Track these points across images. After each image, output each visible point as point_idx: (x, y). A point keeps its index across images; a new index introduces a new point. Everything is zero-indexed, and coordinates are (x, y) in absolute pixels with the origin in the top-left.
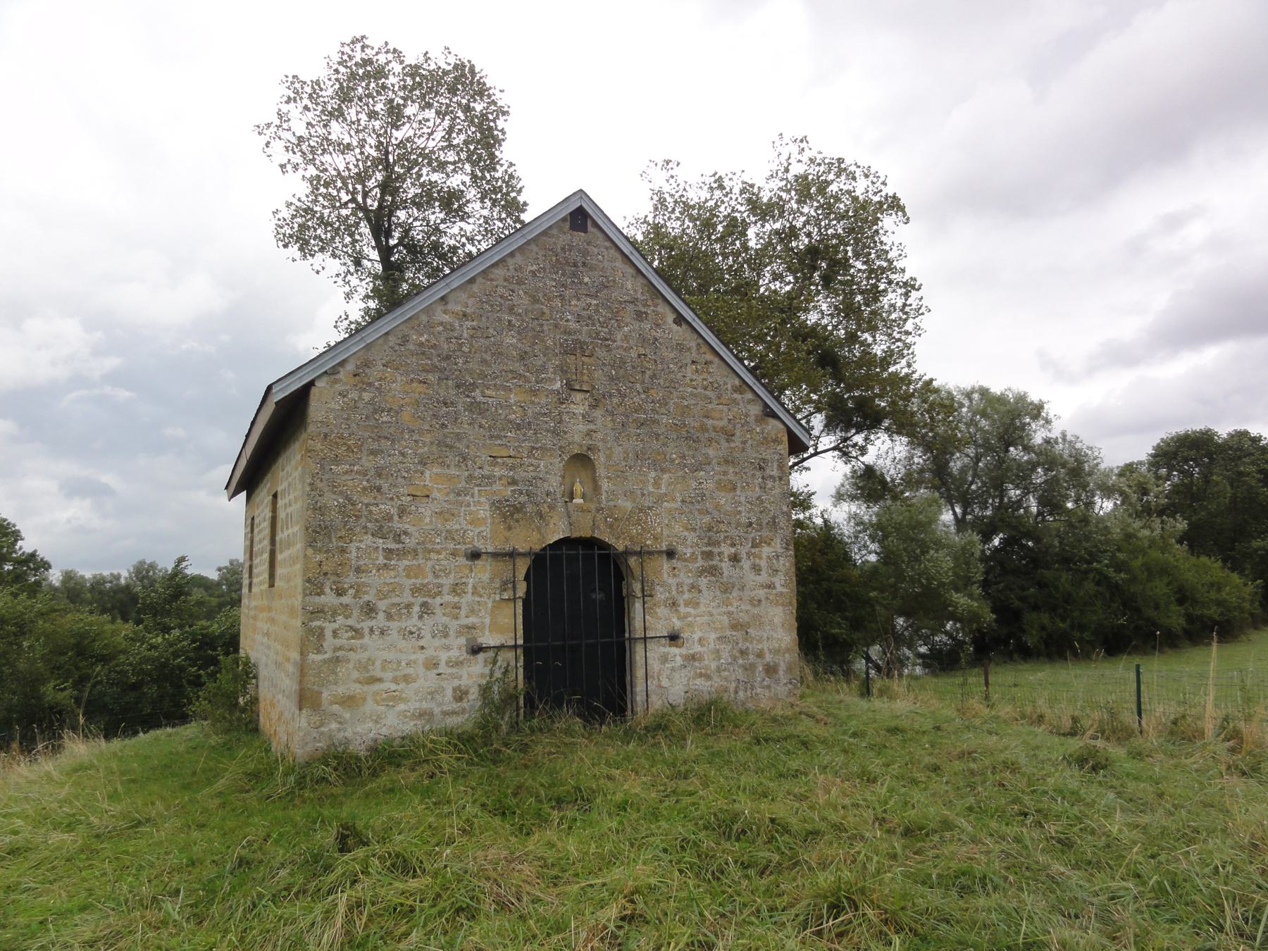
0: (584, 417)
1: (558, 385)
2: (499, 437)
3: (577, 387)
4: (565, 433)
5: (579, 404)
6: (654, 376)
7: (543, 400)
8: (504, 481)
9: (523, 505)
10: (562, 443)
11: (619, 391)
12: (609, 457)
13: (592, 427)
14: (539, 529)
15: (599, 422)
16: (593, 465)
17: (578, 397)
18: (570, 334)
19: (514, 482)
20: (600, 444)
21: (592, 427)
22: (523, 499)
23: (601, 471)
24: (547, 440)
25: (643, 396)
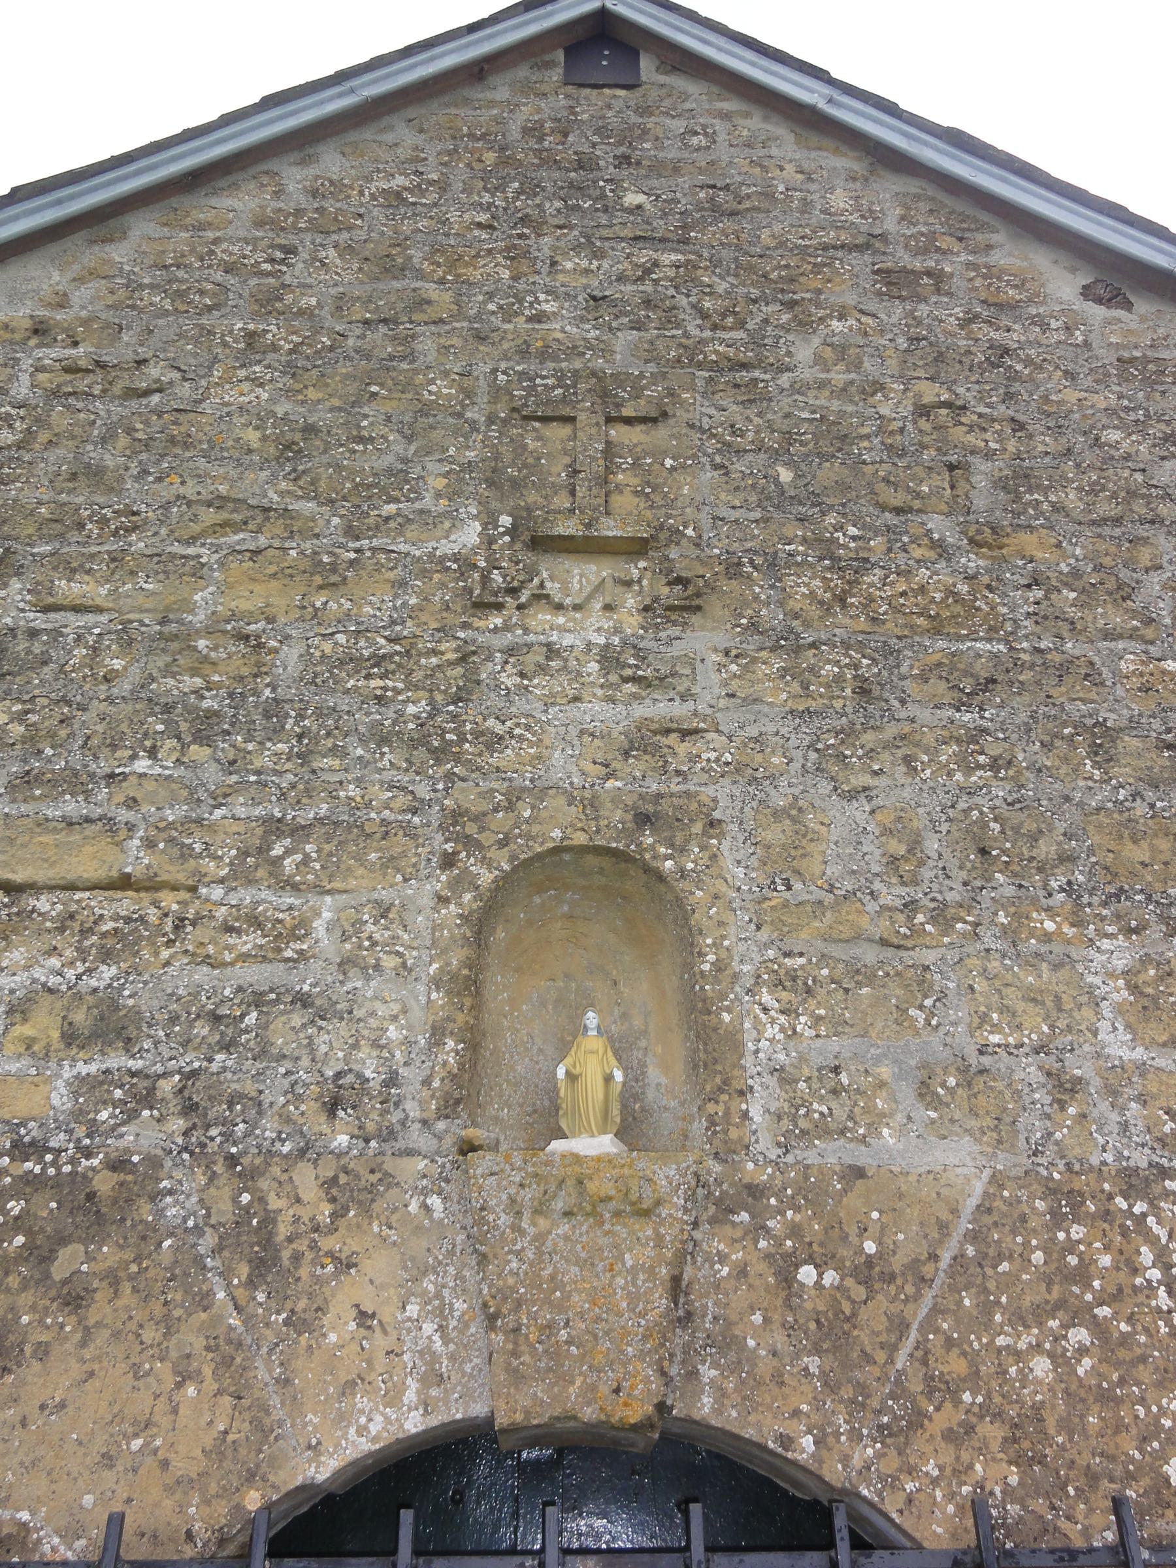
0: (609, 659)
1: (470, 535)
2: (75, 783)
3: (568, 527)
4: (494, 742)
5: (587, 613)
6: (1017, 481)
7: (376, 604)
8: (44, 1024)
9: (137, 1177)
10: (467, 796)
11: (827, 549)
12: (783, 866)
13: (660, 708)
14: (228, 1356)
15: (710, 685)
16: (681, 912)
17: (579, 576)
18: (544, 355)
19: (111, 1026)
20: (724, 796)
21: (660, 708)
22: (142, 1136)
23: (736, 941)
24: (374, 783)
25: (973, 562)
